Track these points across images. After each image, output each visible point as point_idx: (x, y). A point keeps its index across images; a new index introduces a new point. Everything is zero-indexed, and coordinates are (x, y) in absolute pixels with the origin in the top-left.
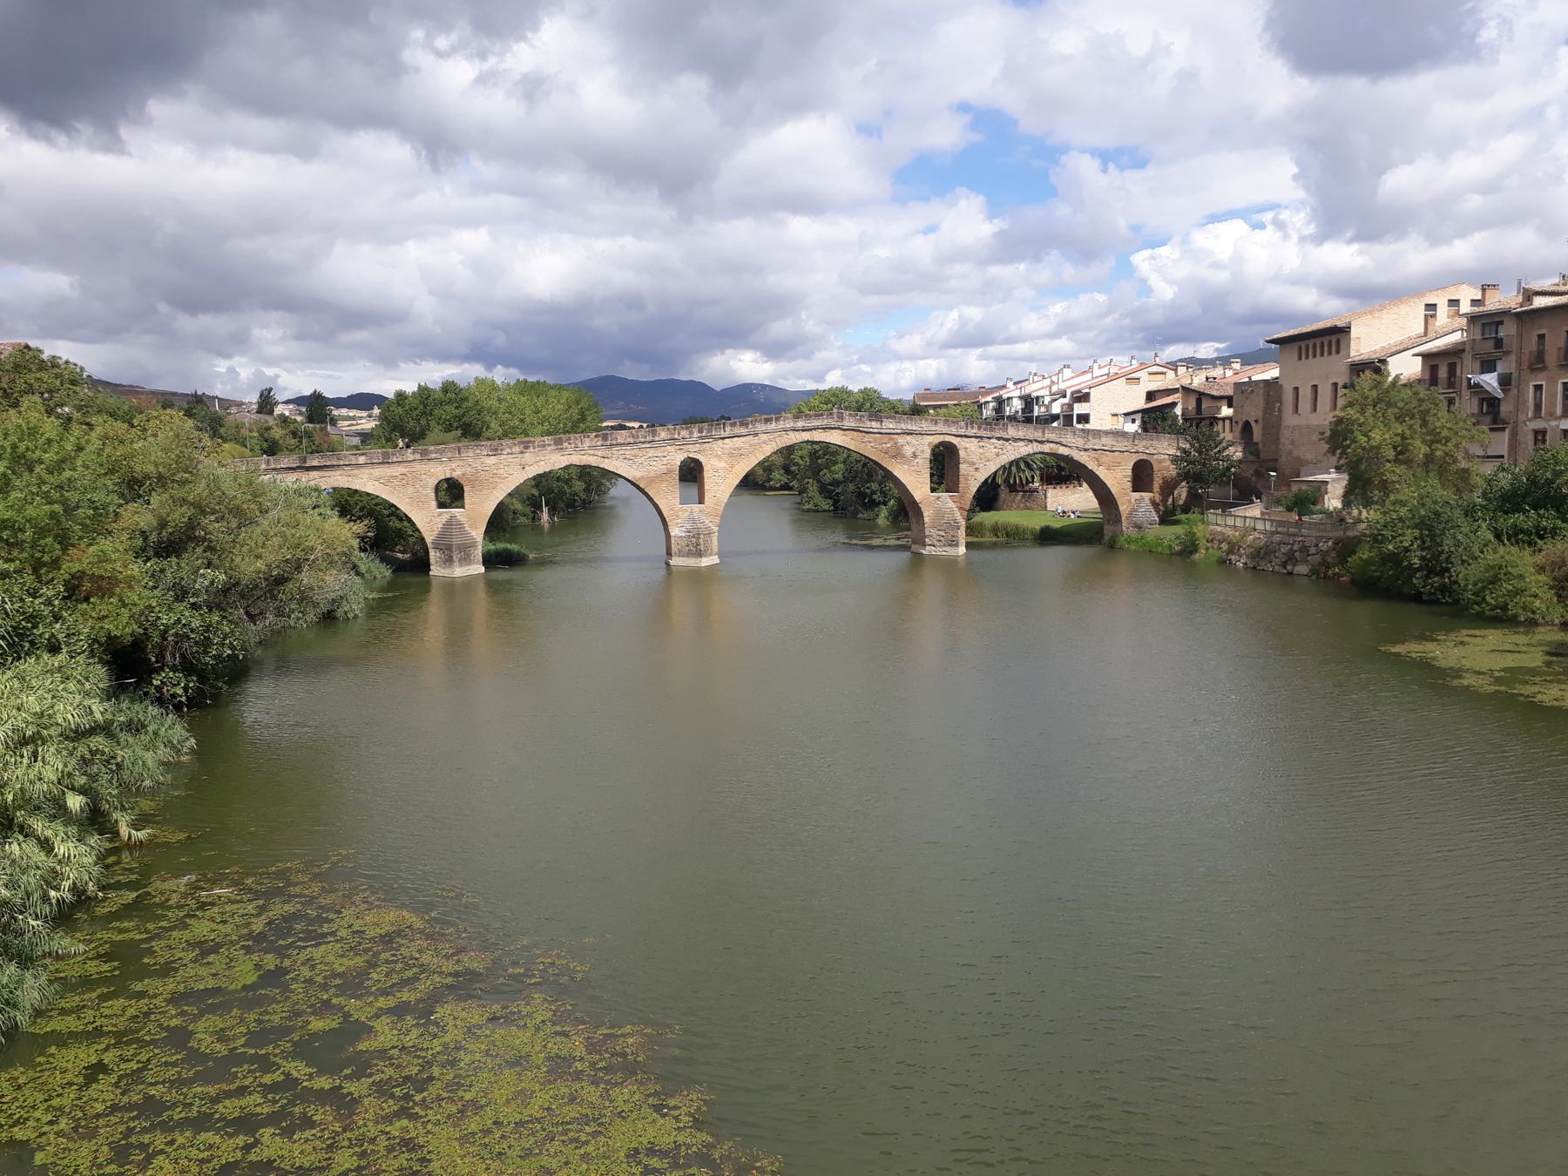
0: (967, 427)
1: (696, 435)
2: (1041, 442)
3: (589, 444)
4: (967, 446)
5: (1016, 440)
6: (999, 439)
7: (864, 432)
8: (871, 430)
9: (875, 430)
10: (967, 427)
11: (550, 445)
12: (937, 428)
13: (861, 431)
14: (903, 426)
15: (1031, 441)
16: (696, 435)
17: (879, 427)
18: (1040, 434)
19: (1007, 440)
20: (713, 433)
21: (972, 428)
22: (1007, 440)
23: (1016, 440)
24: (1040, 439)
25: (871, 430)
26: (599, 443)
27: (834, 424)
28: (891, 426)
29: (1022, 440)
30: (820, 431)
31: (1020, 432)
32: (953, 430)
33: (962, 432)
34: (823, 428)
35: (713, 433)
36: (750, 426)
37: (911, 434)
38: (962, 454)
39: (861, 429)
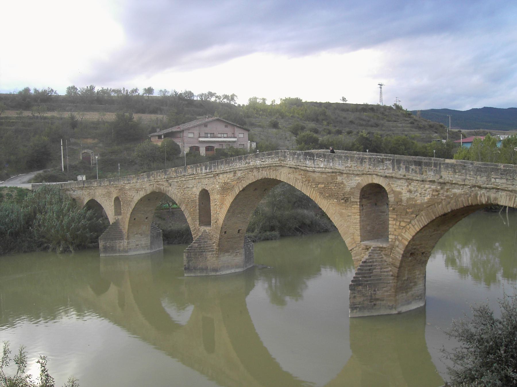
1: (204, 171)
4: (398, 189)
8: (308, 169)
16: (204, 171)
18: (484, 178)
21: (399, 168)
25: (308, 169)
31: (457, 176)
32: (380, 169)
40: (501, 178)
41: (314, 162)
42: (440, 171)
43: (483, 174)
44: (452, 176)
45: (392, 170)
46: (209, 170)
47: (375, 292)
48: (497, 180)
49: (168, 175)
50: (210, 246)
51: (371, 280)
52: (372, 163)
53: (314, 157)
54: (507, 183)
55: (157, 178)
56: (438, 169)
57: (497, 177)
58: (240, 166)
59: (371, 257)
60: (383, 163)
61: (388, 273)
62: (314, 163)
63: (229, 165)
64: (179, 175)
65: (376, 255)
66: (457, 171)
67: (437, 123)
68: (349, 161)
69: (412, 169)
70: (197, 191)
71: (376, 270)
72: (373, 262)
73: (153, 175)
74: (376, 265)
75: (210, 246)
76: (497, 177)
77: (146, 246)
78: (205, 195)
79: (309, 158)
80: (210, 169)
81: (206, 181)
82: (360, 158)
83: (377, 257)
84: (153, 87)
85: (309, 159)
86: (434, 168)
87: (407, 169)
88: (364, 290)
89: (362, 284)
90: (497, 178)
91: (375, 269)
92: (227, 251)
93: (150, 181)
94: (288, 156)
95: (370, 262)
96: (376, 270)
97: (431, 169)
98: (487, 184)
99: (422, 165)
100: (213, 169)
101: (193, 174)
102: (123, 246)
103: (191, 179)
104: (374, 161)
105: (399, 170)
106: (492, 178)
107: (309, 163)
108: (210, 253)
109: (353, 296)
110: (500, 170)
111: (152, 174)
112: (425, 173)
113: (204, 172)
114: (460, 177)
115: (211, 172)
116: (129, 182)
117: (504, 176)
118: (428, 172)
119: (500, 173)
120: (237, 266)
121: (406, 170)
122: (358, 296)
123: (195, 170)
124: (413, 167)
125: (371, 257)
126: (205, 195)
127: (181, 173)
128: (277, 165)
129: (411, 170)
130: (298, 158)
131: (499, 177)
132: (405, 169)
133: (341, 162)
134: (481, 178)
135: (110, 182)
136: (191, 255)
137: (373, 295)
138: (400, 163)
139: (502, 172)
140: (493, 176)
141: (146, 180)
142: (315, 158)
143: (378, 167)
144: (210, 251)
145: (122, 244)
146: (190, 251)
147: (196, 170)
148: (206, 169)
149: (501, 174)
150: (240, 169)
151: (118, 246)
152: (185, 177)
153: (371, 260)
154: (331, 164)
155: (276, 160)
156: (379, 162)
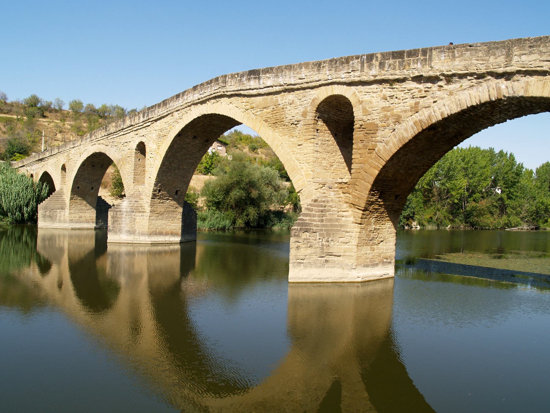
0: (362, 66)
2: (507, 76)
4: (367, 98)
5: (449, 78)
6: (418, 79)
7: (245, 96)
8: (251, 92)
10: (362, 66)
11: (88, 138)
12: (321, 76)
13: (245, 96)
14: (281, 81)
15: (481, 76)
17: (257, 86)
18: (502, 59)
19: (433, 80)
20: (150, 116)
21: (370, 67)
22: (433, 80)
23: (449, 78)
24: (500, 70)
27: (221, 91)
29: (462, 76)
30: (213, 101)
31: (457, 62)
33: (355, 77)
34: (215, 98)
35: (150, 116)
36: (168, 106)
37: (293, 90)
38: (358, 113)
39: (242, 92)
40: (531, 53)
41: (259, 81)
42: (430, 59)
43: (498, 53)
44: (450, 63)
45: (361, 72)
46: (146, 117)
47: (327, 243)
48: (524, 58)
50: (141, 207)
51: (323, 226)
52: (333, 67)
53: (259, 74)
54: (542, 59)
56: (428, 57)
57: (524, 52)
58: (178, 106)
59: (325, 195)
60: (348, 63)
61: (349, 219)
62: (259, 82)
63: (166, 107)
65: (332, 193)
66: (457, 55)
68: (303, 69)
69: (390, 65)
70: (134, 145)
71: (331, 213)
72: (328, 202)
74: (330, 206)
75: (141, 207)
76: (524, 52)
77: (92, 219)
79: (254, 77)
81: (142, 132)
82: (317, 63)
83: (333, 196)
85: (254, 78)
86: (422, 58)
87: (382, 65)
88: (312, 238)
89: (311, 229)
90: (523, 55)
91: (329, 211)
92: (161, 214)
93: (92, 142)
94: (229, 80)
95: (324, 202)
96: (331, 213)
97: (417, 60)
98: (506, 67)
99: (404, 56)
100: (150, 115)
102: (64, 215)
103: (129, 131)
104: (336, 63)
105: (371, 70)
106: (516, 55)
107: (253, 83)
108: (140, 214)
109: (296, 246)
110: (529, 41)
111: (94, 133)
112: (407, 67)
114: (461, 63)
115: (148, 119)
116: (74, 146)
117: (535, 49)
118: (412, 64)
119: (528, 45)
120: (173, 234)
121: (380, 68)
122: (304, 246)
123: (133, 120)
124: (391, 61)
125: (325, 195)
127: (120, 126)
128: (216, 95)
129: (387, 66)
130: (241, 79)
131: (526, 52)
132: (379, 66)
133: (292, 73)
134: (496, 59)
135: (59, 149)
136: (116, 215)
137: (325, 247)
138: (372, 60)
139: (531, 43)
140: (515, 53)
141: (88, 140)
142: (261, 76)
143: (341, 70)
144: (140, 212)
145: (62, 214)
146: (116, 210)
149: (530, 47)
150: (178, 109)
151: (58, 215)
152: (124, 130)
153: (324, 199)
155: (215, 89)
156: (342, 63)
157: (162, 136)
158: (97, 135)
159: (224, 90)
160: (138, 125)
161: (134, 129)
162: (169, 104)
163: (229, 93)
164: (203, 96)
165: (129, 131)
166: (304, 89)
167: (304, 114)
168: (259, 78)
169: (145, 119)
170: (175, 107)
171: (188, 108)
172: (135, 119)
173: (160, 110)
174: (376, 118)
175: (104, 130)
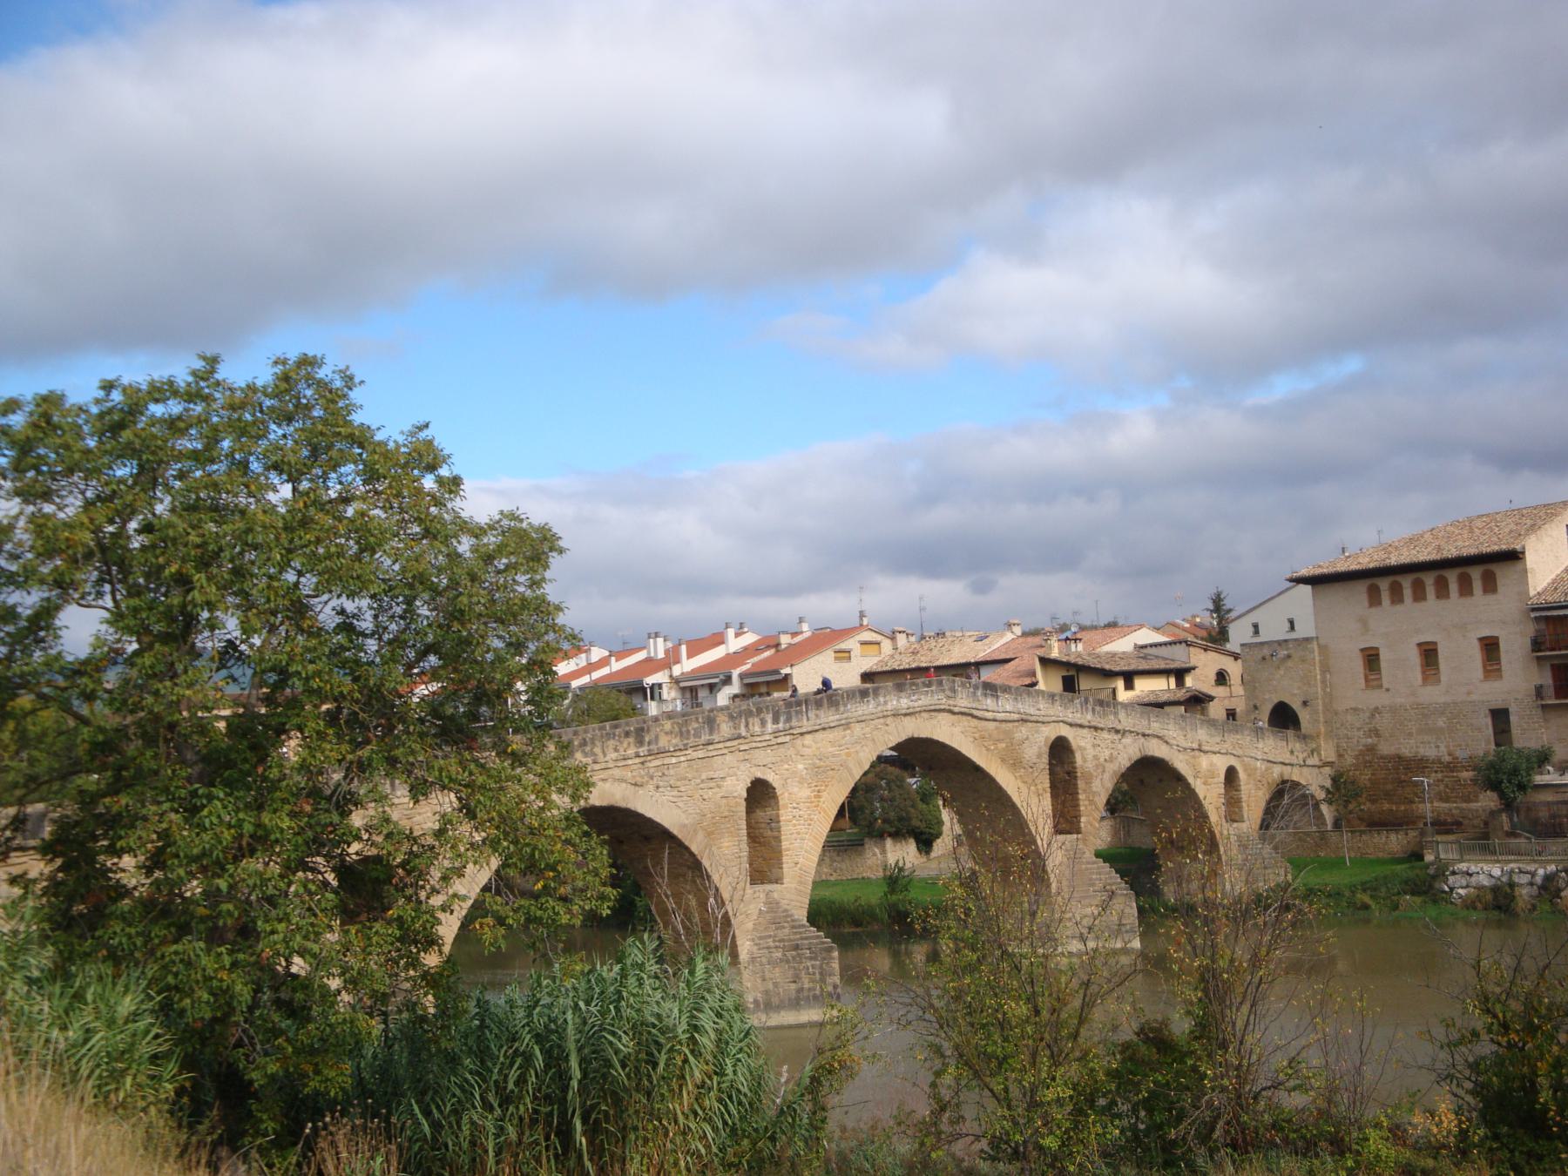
1: (770, 727)
3: (614, 755)
9: (989, 715)
16: (770, 727)
17: (996, 709)
26: (631, 752)
28: (1008, 708)
36: (842, 709)
39: (975, 712)
46: (785, 722)
49: (649, 743)
55: (605, 755)
64: (691, 741)
67: (1009, 636)
73: (588, 749)
78: (760, 794)
80: (788, 720)
81: (763, 756)
84: (1491, 598)
101: (740, 737)
107: (989, 702)
113: (770, 730)
115: (791, 728)
126: (760, 794)
127: (697, 735)
147: (747, 725)
148: (776, 720)
152: (711, 747)
154: (1020, 706)
157: (820, 772)
158: (598, 750)
159: (951, 702)
160: (759, 739)
161: (742, 748)
162: (845, 705)
163: (956, 710)
164: (916, 704)
165: (715, 753)
166: (1037, 722)
167: (1039, 756)
168: (997, 697)
169: (781, 726)
170: (860, 713)
171: (882, 720)
172: (751, 720)
173: (821, 713)
174: (1090, 765)
175: (631, 740)
